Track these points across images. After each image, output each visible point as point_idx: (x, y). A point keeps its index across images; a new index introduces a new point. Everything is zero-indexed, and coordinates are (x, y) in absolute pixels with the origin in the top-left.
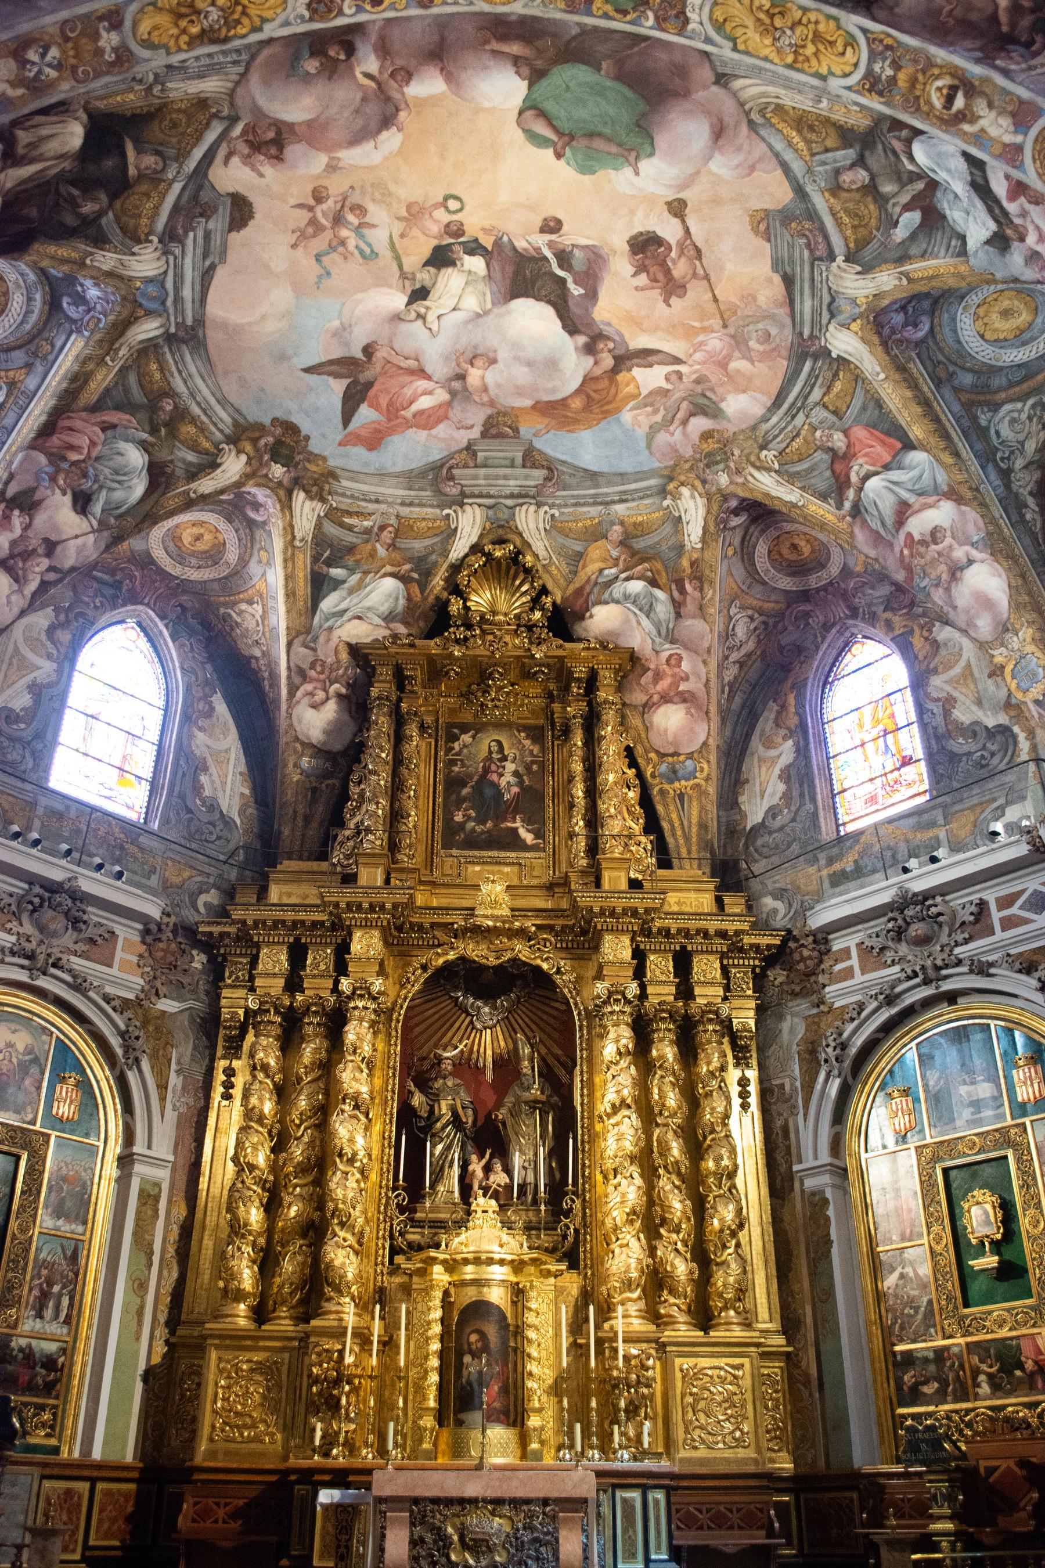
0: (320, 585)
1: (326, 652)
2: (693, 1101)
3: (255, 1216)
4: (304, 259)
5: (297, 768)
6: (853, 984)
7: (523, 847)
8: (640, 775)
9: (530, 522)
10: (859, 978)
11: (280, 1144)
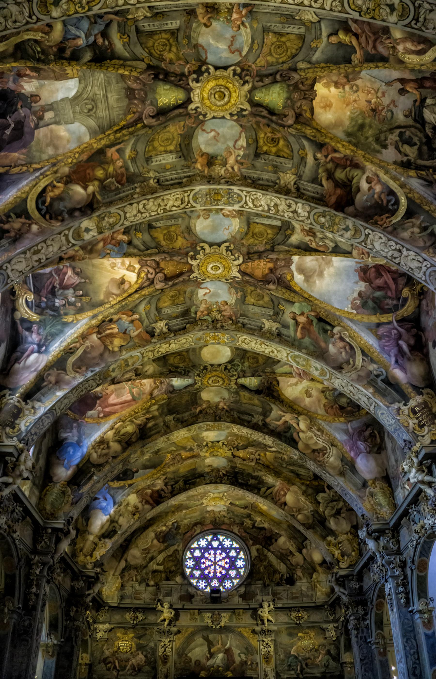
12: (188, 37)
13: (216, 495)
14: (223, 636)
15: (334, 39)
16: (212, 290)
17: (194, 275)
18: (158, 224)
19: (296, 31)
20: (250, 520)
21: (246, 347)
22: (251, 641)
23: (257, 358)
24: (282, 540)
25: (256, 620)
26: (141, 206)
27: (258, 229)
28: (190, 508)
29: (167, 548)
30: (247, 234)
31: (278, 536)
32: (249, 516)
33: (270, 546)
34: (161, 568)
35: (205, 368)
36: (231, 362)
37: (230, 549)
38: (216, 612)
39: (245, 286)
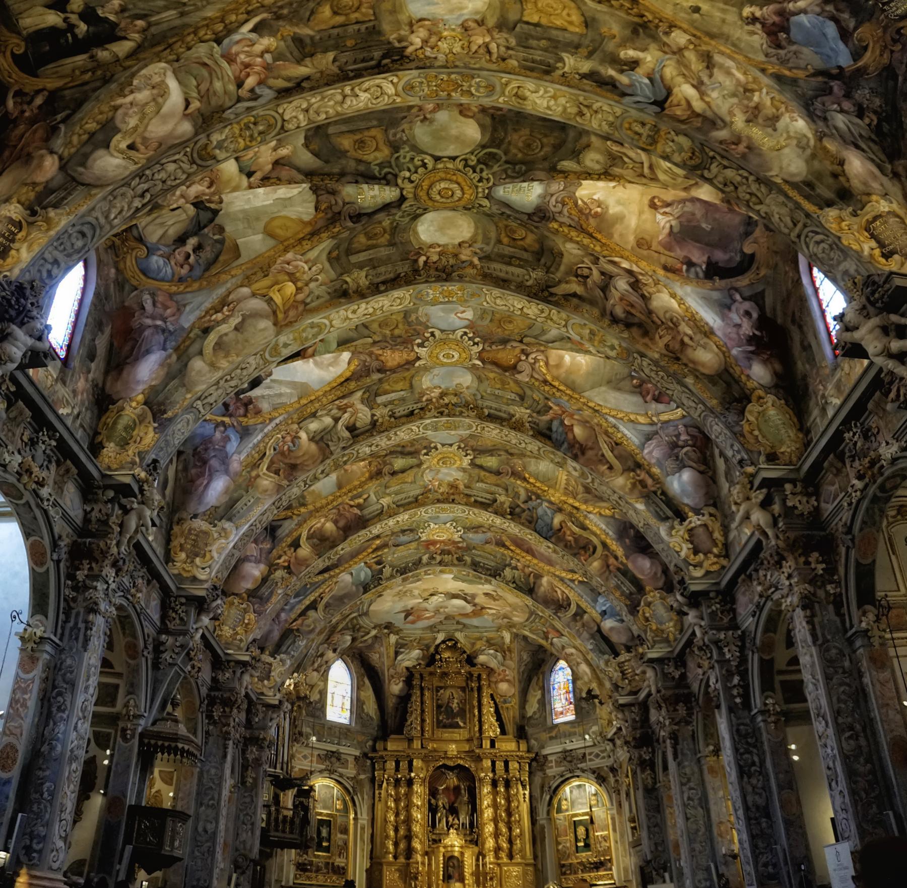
0: (397, 654)
1: (399, 670)
2: (508, 800)
3: (392, 833)
4: (397, 599)
5: (391, 703)
6: (553, 770)
7: (460, 727)
8: (495, 703)
9: (459, 636)
10: (555, 769)
11: (397, 815)
12: (470, 476)
15: (365, 496)
16: (453, 316)
17: (476, 349)
18: (513, 396)
19: (392, 489)
21: (396, 293)
23: (369, 238)
26: (523, 445)
27: (400, 386)
30: (412, 377)
35: (465, 208)
36: (416, 217)
39: (406, 332)
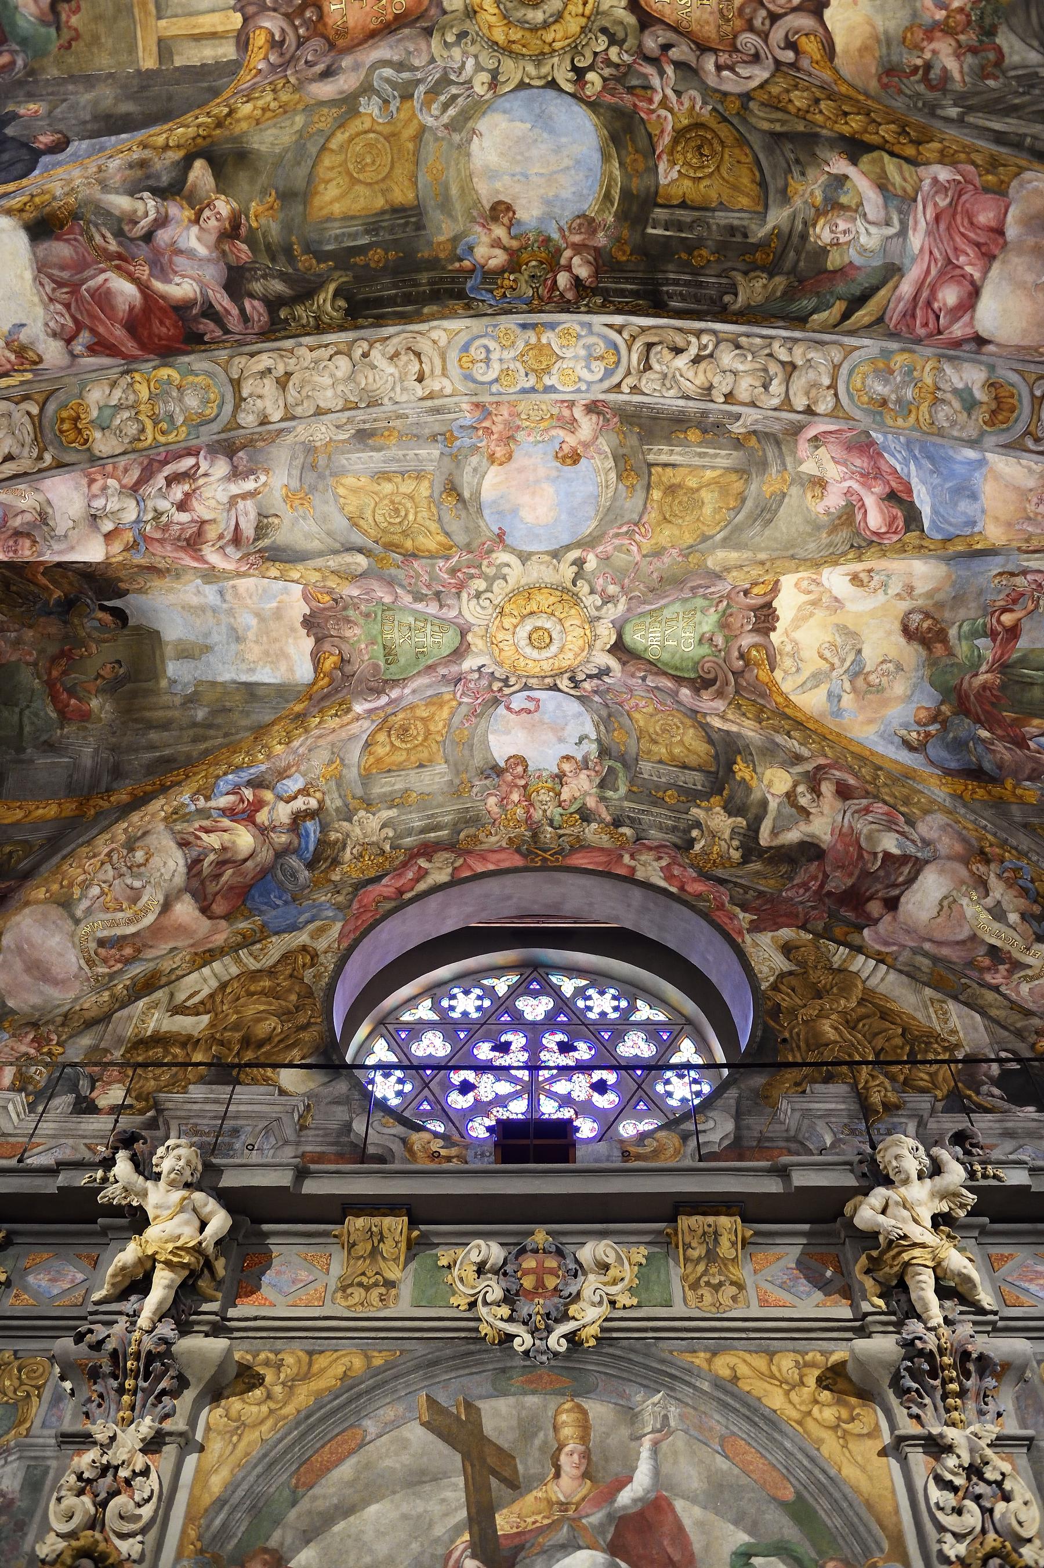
13: (539, 572)
14: (598, 1410)
20: (732, 809)
22: (830, 1446)
24: (927, 894)
25: (848, 1292)
28: (395, 683)
29: (247, 941)
31: (906, 868)
32: (721, 771)
33: (860, 929)
34: (195, 1025)
37: (621, 1027)
38: (540, 1236)
